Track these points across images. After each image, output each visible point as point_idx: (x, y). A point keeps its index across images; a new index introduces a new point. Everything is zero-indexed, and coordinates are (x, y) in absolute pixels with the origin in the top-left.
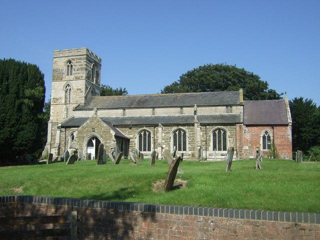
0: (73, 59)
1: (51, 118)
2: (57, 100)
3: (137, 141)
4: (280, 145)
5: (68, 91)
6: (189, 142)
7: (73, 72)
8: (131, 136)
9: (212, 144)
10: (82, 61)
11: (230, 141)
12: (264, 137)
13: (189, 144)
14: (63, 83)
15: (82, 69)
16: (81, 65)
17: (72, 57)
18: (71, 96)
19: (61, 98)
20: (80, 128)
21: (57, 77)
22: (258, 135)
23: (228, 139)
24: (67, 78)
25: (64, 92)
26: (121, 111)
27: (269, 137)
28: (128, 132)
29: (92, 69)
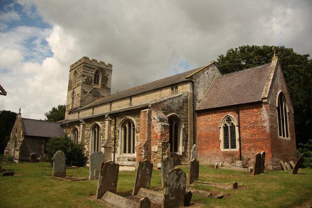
10: (81, 69)
12: (226, 128)
22: (216, 125)
27: (233, 127)
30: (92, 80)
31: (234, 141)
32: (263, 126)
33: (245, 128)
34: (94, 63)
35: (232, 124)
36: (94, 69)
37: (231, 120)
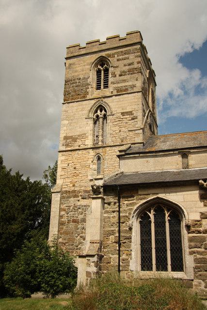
0: (109, 56)
2: (75, 139)
7: (111, 79)
10: (131, 56)
15: (131, 72)
16: (129, 65)
19: (83, 136)
25: (91, 122)
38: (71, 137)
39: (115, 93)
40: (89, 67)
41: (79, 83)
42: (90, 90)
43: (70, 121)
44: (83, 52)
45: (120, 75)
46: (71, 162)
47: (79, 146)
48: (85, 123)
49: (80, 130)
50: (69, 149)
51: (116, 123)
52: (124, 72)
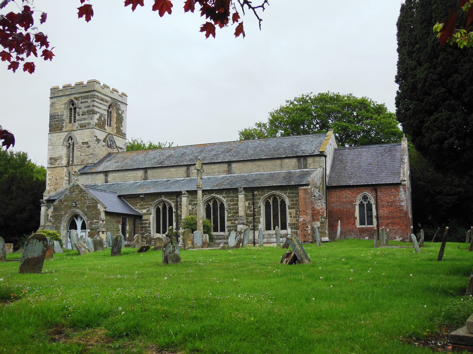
0: (76, 99)
1: (48, 188)
2: (55, 160)
3: (152, 218)
4: (388, 218)
5: (71, 146)
6: (228, 217)
7: (77, 118)
8: (144, 211)
9: (262, 219)
11: (290, 214)
12: (361, 205)
13: (228, 220)
14: (63, 135)
16: (88, 107)
17: (76, 96)
18: (75, 155)
19: (60, 158)
20: (56, 203)
21: (54, 126)
23: (288, 211)
24: (69, 127)
26: (141, 173)
27: (369, 205)
28: (140, 206)
29: (109, 113)
30: (105, 119)
31: (370, 217)
32: (400, 206)
33: (383, 206)
34: (105, 91)
35: (369, 202)
36: (107, 102)
37: (367, 198)
38: (54, 158)
39: (79, 128)
40: (63, 106)
41: (58, 118)
42: (64, 124)
43: (53, 147)
44: (60, 94)
45: (82, 115)
46: (54, 175)
47: (58, 165)
48: (61, 149)
49: (59, 153)
50: (53, 166)
51: (79, 150)
52: (84, 112)
